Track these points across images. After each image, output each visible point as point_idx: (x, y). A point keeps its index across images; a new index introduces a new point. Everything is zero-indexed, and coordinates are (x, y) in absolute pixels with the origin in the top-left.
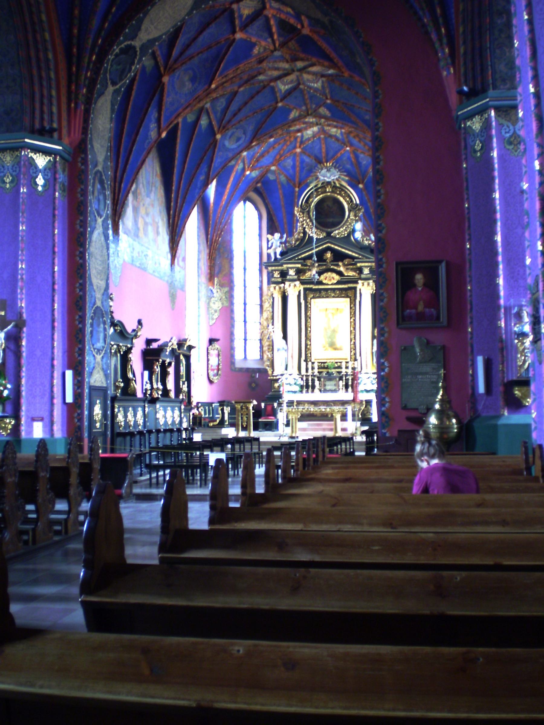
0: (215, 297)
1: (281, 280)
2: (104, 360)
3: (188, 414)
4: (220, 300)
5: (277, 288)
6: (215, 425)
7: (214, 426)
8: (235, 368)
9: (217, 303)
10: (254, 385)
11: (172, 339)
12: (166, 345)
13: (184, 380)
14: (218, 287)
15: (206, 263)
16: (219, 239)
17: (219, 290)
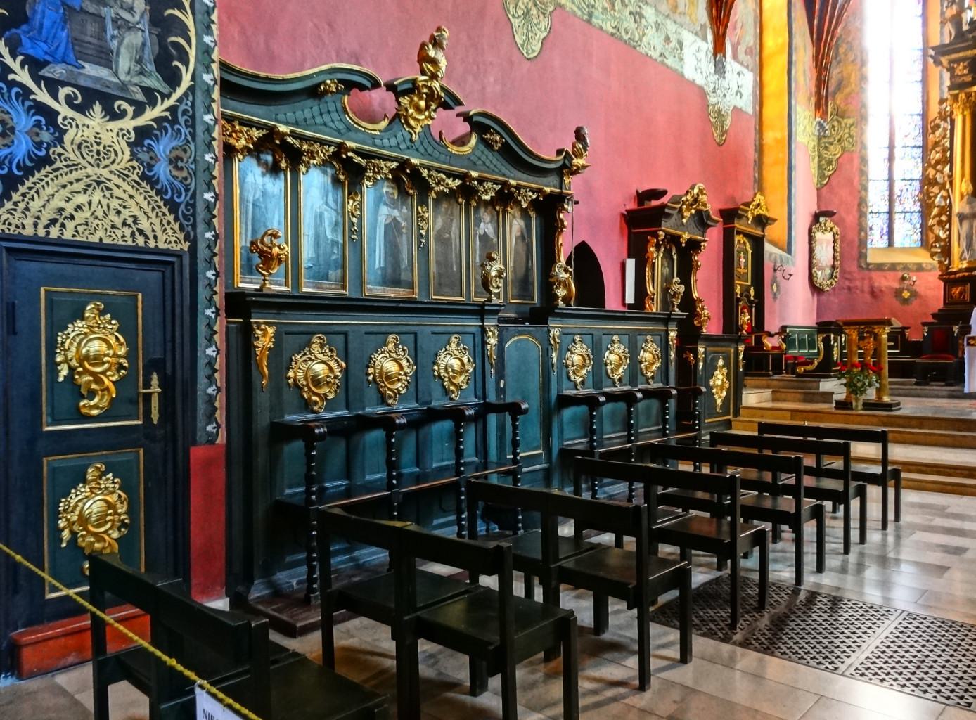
0: (828, 137)
1: (970, 79)
2: (164, 147)
3: (733, 350)
4: (839, 140)
5: (962, 96)
6: (809, 371)
7: (806, 374)
8: (868, 265)
9: (832, 147)
10: (906, 294)
11: (692, 188)
12: (676, 200)
13: (749, 283)
14: (835, 117)
15: (808, 73)
16: (836, 28)
17: (836, 124)
